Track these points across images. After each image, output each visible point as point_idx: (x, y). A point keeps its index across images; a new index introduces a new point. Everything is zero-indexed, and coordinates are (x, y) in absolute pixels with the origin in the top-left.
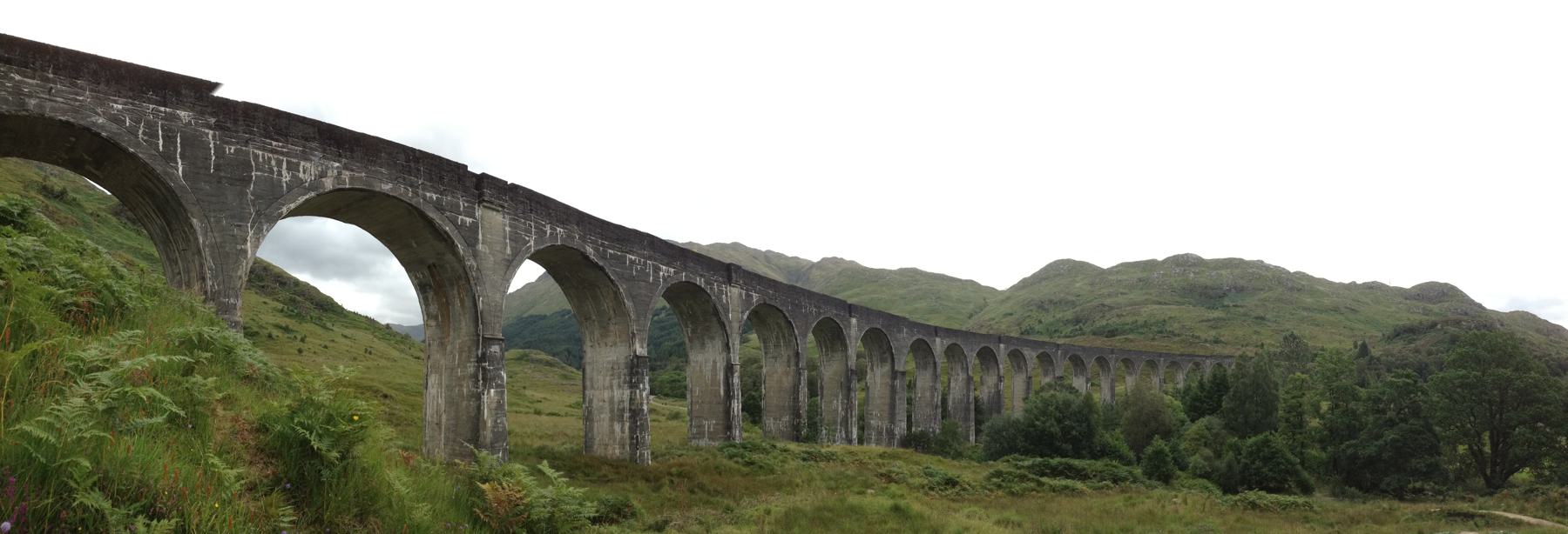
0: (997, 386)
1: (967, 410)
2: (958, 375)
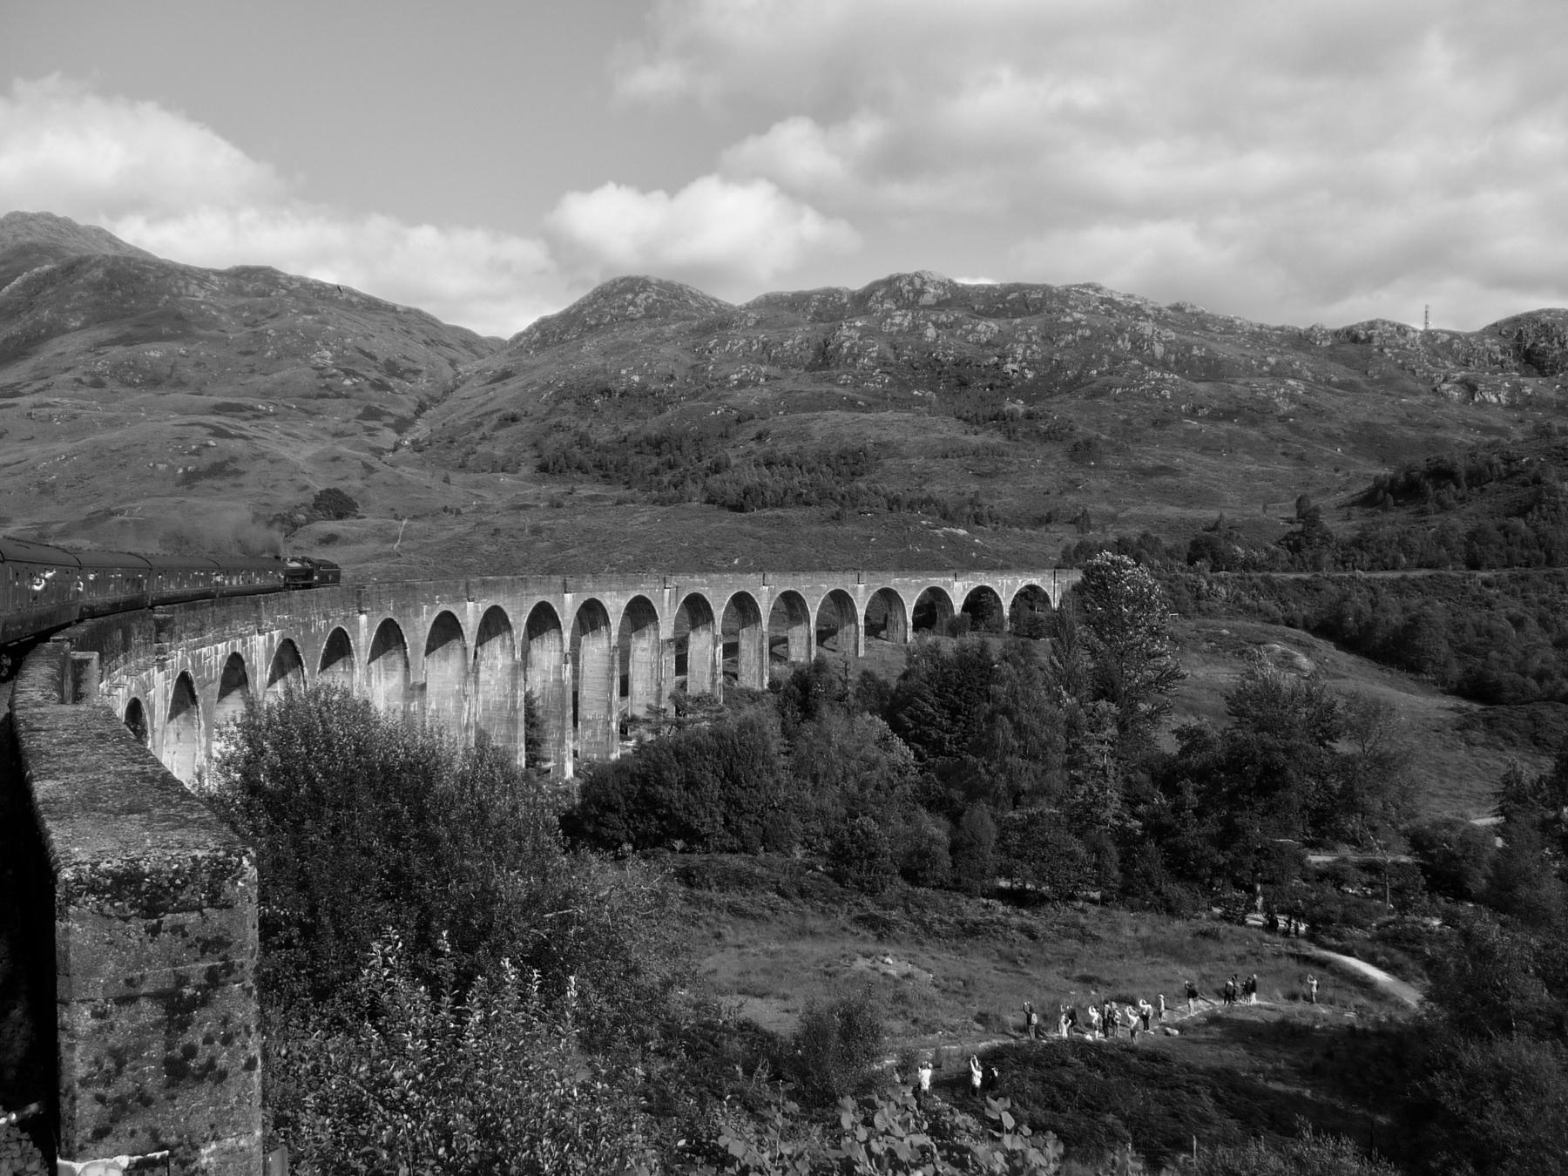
0: (559, 670)
1: (512, 722)
2: (495, 658)
